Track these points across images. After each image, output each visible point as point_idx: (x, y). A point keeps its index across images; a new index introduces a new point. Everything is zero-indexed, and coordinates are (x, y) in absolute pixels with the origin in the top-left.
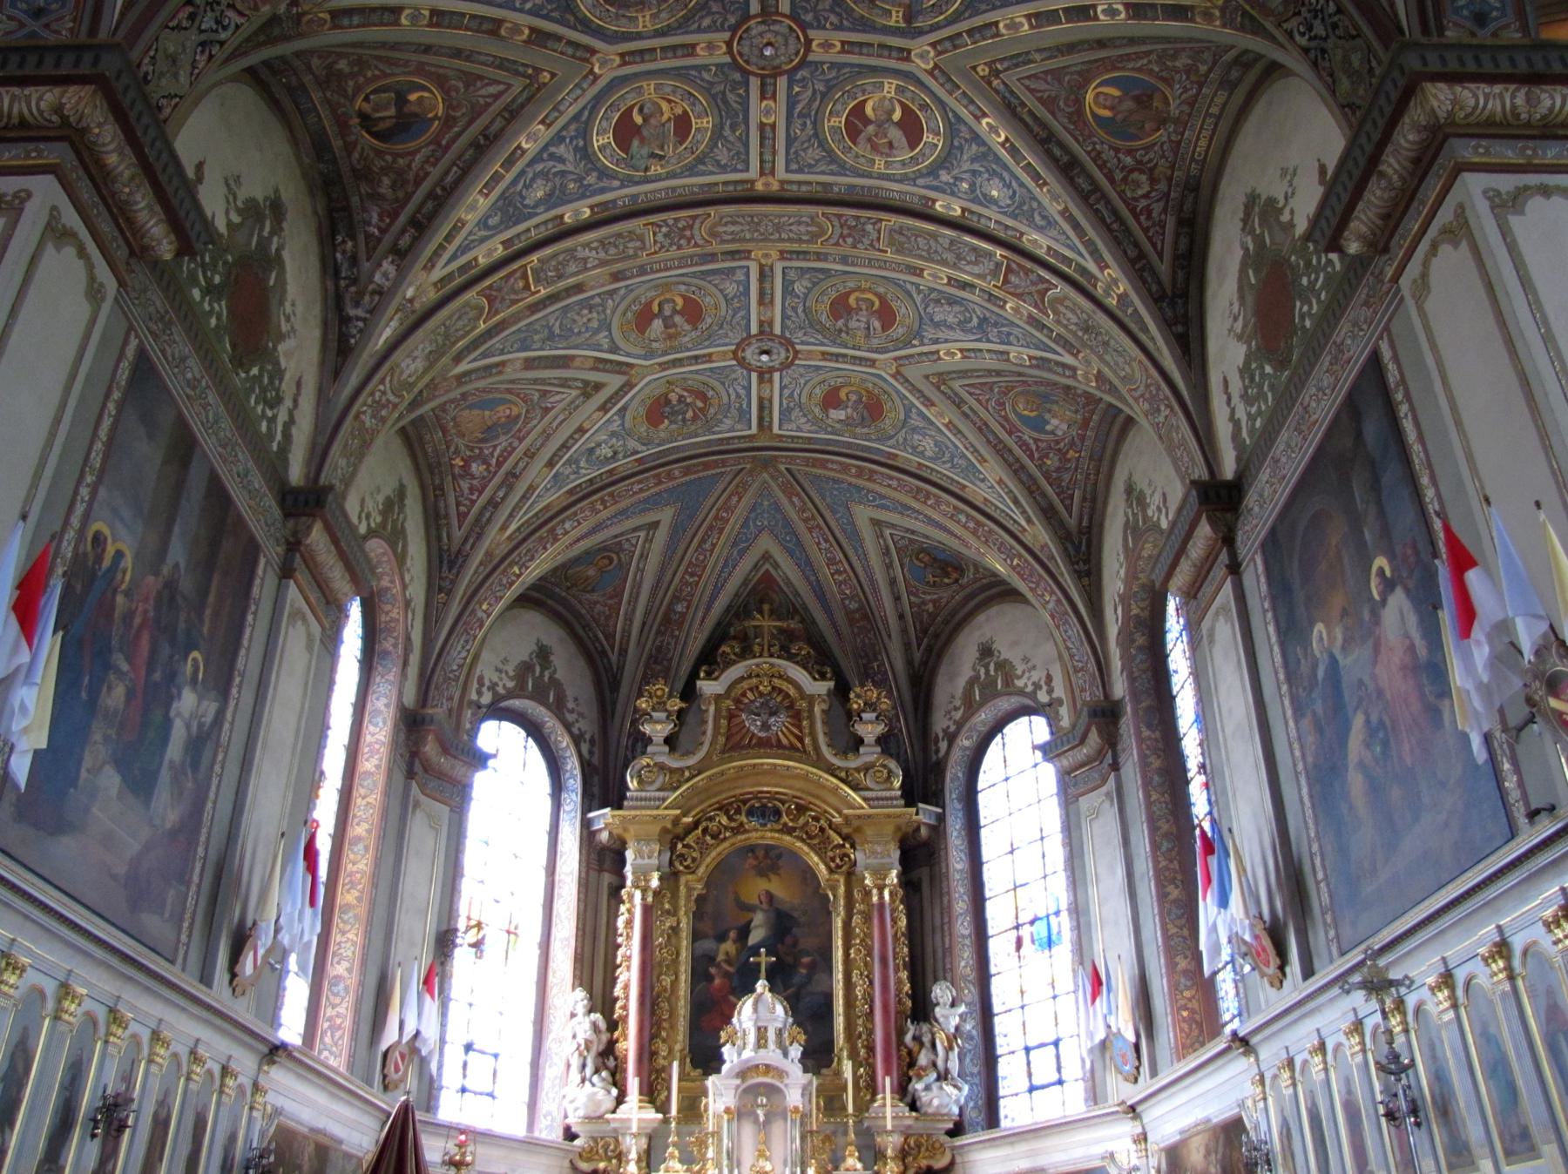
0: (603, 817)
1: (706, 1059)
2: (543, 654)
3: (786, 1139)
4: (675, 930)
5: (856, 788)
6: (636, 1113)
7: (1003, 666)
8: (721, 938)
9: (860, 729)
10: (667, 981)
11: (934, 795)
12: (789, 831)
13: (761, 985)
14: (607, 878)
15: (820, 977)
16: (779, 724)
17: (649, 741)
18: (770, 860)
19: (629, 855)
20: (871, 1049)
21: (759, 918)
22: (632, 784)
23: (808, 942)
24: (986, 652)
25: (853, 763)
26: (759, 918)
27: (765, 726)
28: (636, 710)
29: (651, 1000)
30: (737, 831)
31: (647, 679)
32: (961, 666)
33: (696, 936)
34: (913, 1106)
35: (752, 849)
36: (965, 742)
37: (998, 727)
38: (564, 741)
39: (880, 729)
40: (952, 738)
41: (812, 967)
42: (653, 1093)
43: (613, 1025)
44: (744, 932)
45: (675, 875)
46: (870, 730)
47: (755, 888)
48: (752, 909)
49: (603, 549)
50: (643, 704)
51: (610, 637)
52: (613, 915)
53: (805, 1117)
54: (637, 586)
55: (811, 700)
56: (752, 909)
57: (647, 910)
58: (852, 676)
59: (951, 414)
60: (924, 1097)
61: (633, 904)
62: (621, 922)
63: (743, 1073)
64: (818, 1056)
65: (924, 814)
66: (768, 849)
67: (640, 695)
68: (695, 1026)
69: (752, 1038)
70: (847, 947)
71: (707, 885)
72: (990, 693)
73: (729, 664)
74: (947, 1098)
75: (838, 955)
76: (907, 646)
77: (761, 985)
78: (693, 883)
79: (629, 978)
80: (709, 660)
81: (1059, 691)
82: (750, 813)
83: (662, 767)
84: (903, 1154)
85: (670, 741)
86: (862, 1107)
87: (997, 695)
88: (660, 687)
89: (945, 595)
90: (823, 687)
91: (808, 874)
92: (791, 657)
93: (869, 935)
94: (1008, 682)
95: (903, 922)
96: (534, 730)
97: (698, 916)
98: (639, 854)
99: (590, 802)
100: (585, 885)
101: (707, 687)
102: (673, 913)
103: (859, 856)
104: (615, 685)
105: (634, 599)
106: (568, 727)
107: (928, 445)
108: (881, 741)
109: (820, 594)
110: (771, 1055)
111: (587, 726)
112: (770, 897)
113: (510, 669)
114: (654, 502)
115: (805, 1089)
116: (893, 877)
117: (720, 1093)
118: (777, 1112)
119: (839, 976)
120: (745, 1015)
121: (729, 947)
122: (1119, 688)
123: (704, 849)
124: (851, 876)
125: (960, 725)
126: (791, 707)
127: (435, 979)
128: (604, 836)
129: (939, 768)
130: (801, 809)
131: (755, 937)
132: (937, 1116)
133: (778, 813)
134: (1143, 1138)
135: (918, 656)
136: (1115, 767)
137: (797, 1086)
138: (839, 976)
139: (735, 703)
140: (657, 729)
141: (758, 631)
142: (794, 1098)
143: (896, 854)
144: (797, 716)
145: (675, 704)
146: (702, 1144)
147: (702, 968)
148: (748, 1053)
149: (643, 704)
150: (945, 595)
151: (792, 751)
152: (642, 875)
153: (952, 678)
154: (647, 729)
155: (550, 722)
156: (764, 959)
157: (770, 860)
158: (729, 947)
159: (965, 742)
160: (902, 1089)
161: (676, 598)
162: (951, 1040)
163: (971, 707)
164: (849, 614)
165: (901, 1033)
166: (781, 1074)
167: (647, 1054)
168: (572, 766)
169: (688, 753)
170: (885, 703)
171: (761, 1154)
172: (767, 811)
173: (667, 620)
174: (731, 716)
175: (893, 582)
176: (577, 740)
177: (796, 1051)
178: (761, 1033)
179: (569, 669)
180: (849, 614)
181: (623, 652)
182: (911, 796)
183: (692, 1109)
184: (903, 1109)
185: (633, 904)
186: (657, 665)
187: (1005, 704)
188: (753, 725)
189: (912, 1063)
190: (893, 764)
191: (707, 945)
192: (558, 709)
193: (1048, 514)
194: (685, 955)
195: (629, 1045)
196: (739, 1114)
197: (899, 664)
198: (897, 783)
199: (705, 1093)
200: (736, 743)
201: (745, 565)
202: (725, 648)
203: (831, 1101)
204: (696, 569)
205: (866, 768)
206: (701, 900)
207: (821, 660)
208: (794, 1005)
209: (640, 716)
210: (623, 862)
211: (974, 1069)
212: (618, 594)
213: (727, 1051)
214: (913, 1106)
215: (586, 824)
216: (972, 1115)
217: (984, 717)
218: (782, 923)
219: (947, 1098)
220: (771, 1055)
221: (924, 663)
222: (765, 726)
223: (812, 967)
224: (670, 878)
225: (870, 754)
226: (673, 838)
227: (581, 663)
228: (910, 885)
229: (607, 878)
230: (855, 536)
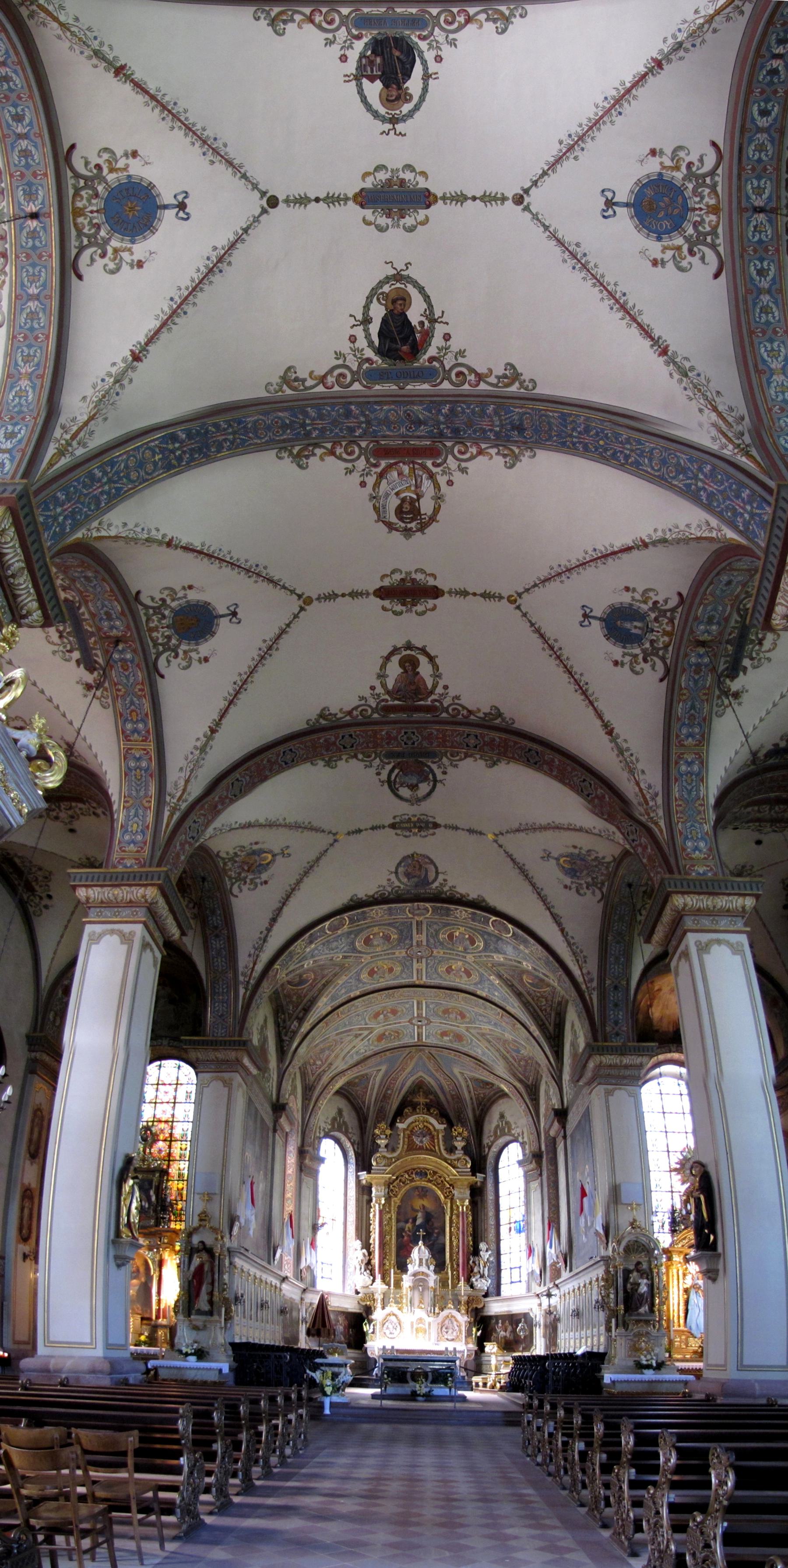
0: (363, 1175)
1: (402, 1267)
2: (340, 1112)
3: (428, 1296)
4: (390, 1218)
5: (454, 1167)
6: (379, 1286)
7: (507, 1123)
8: (407, 1222)
9: (457, 1144)
10: (388, 1237)
11: (483, 1170)
12: (430, 1181)
13: (420, 1243)
14: (366, 1197)
15: (441, 1237)
16: (425, 1141)
17: (379, 1146)
18: (424, 1192)
19: (373, 1190)
20: (458, 1265)
21: (420, 1215)
22: (374, 1163)
23: (437, 1224)
24: (502, 1116)
25: (453, 1157)
26: (420, 1215)
27: (421, 1142)
28: (374, 1134)
29: (382, 1245)
30: (412, 1180)
31: (379, 1122)
32: (492, 1123)
33: (398, 1221)
34: (472, 1286)
35: (417, 1188)
36: (494, 1149)
37: (506, 1145)
38: (348, 1145)
39: (463, 1144)
40: (490, 1147)
41: (438, 1234)
42: (384, 1279)
43: (370, 1254)
44: (415, 1220)
45: (390, 1197)
46: (459, 1144)
47: (418, 1203)
48: (417, 1211)
49: (363, 1076)
50: (377, 1131)
51: (364, 1103)
52: (369, 1212)
53: (435, 1290)
54: (374, 1085)
55: (437, 1131)
56: (417, 1211)
57: (381, 1212)
58: (454, 1121)
59: (487, 1044)
60: (475, 1283)
61: (375, 1209)
62: (371, 1215)
63: (415, 1275)
64: (440, 1267)
65: (480, 1176)
66: (423, 1188)
67: (375, 1128)
68: (398, 1255)
69: (417, 1262)
70: (451, 1227)
71: (402, 1201)
72: (503, 1134)
73: (408, 1116)
74: (483, 1284)
75: (447, 1229)
76: (474, 1110)
77: (420, 1243)
78: (396, 1201)
79: (375, 1237)
80: (399, 1113)
81: (526, 1139)
82: (417, 1174)
83: (384, 1157)
84: (468, 1303)
85: (386, 1146)
86: (454, 1286)
87: (505, 1134)
88: (383, 1125)
89: (487, 1091)
90: (441, 1127)
91: (437, 1198)
92: (431, 1115)
93: (458, 1223)
94: (509, 1130)
95: (470, 1219)
96: (338, 1141)
97: (398, 1213)
98: (377, 1190)
99: (357, 1170)
100: (358, 1200)
101: (401, 1126)
102: (389, 1212)
103: (455, 1192)
104: (366, 1121)
105: (372, 1089)
106: (349, 1139)
107: (480, 1051)
108: (464, 1148)
109: (442, 1088)
110: (424, 1269)
111: (356, 1138)
112: (424, 1206)
113: (329, 1121)
114: (380, 1064)
115: (435, 1281)
116: (467, 1203)
117: (407, 1281)
118: (425, 1287)
119: (448, 1237)
120: (415, 1254)
121: (409, 1225)
122: (543, 1148)
123: (400, 1188)
124: (452, 1200)
125: (493, 1142)
126: (430, 1134)
127: (313, 1244)
128: (364, 1182)
129: (484, 1158)
130: (435, 1173)
131: (419, 1221)
132: (480, 1290)
133: (426, 1174)
134: (540, 1305)
135: (478, 1113)
136: (541, 1175)
137: (432, 1279)
138: (448, 1237)
139: (411, 1132)
140: (382, 1142)
141: (418, 1104)
142: (431, 1284)
143: (468, 1192)
144: (433, 1138)
145: (388, 1132)
146: (401, 1297)
147: (400, 1232)
148: (416, 1268)
149: (377, 1131)
150: (487, 1091)
151: (431, 1151)
152: (378, 1198)
153: (490, 1123)
154: (379, 1142)
155: (343, 1138)
156: (422, 1233)
157: (424, 1192)
158: (409, 1225)
159: (494, 1149)
160: (468, 1280)
161: (388, 1089)
162: (485, 1264)
163: (497, 1137)
164: (452, 1096)
165: (469, 1260)
166: (427, 1275)
167: (382, 1264)
168: (351, 1154)
169: (393, 1150)
170: (466, 1134)
171: (421, 1302)
172: (422, 1173)
173: (384, 1096)
174: (409, 1137)
175: (468, 1086)
176: (353, 1144)
177: (432, 1267)
178: (421, 1260)
179: (350, 1117)
180: (452, 1096)
181: (368, 1108)
182: (474, 1171)
183: (398, 1285)
184: (469, 1288)
185: (375, 1209)
186: (380, 1115)
187: (508, 1138)
188: (417, 1140)
189: (472, 1271)
190: (467, 1158)
191: (402, 1224)
192: (346, 1134)
193: (520, 1081)
194: (394, 1228)
195: (376, 1261)
196: (413, 1288)
197: (471, 1116)
198: (469, 1166)
199: (402, 1280)
200: (412, 1148)
201: (412, 1079)
202: (406, 1110)
203: (444, 1283)
204: (395, 1079)
205: (458, 1159)
206: (399, 1207)
207: (443, 1116)
208: (430, 1247)
209: (374, 1137)
210: (371, 1192)
211: (493, 1273)
212: (367, 1088)
213: (409, 1266)
214: (472, 1286)
215: (357, 1177)
216: (491, 1290)
217: (501, 1141)
218: (428, 1217)
219: (483, 1284)
220: (424, 1269)
221: (480, 1115)
222: (421, 1142)
223: (438, 1234)
224: (388, 1199)
225: (459, 1154)
226: (389, 1184)
227: (353, 1114)
228: (474, 1204)
229: (366, 1197)
230: (455, 1076)
